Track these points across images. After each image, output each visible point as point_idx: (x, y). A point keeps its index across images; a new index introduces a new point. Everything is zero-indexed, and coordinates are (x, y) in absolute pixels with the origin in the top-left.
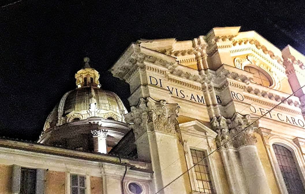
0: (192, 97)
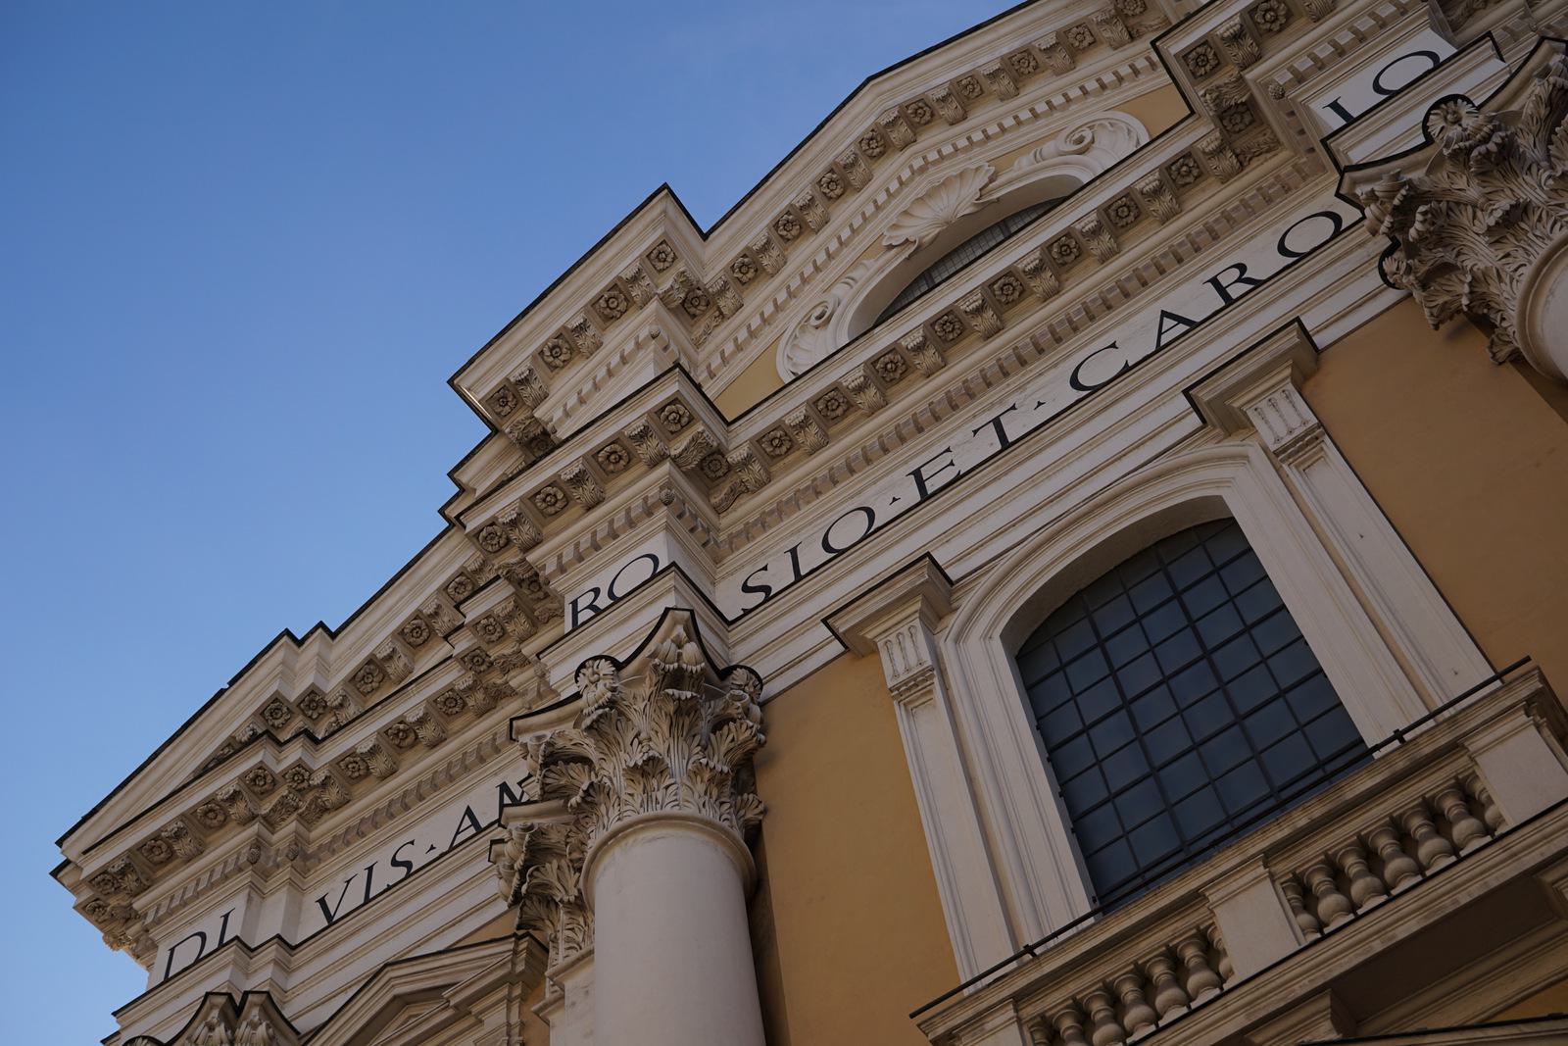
0: (467, 822)
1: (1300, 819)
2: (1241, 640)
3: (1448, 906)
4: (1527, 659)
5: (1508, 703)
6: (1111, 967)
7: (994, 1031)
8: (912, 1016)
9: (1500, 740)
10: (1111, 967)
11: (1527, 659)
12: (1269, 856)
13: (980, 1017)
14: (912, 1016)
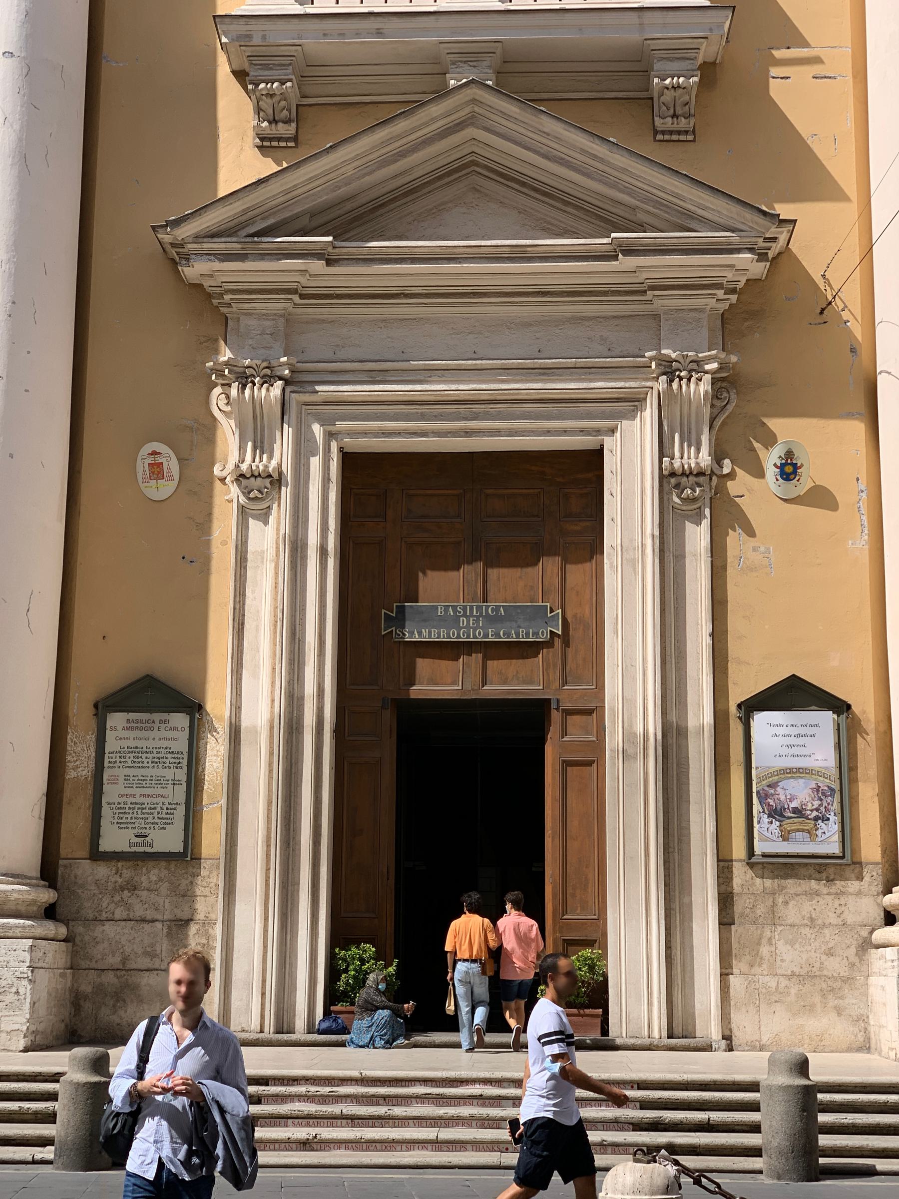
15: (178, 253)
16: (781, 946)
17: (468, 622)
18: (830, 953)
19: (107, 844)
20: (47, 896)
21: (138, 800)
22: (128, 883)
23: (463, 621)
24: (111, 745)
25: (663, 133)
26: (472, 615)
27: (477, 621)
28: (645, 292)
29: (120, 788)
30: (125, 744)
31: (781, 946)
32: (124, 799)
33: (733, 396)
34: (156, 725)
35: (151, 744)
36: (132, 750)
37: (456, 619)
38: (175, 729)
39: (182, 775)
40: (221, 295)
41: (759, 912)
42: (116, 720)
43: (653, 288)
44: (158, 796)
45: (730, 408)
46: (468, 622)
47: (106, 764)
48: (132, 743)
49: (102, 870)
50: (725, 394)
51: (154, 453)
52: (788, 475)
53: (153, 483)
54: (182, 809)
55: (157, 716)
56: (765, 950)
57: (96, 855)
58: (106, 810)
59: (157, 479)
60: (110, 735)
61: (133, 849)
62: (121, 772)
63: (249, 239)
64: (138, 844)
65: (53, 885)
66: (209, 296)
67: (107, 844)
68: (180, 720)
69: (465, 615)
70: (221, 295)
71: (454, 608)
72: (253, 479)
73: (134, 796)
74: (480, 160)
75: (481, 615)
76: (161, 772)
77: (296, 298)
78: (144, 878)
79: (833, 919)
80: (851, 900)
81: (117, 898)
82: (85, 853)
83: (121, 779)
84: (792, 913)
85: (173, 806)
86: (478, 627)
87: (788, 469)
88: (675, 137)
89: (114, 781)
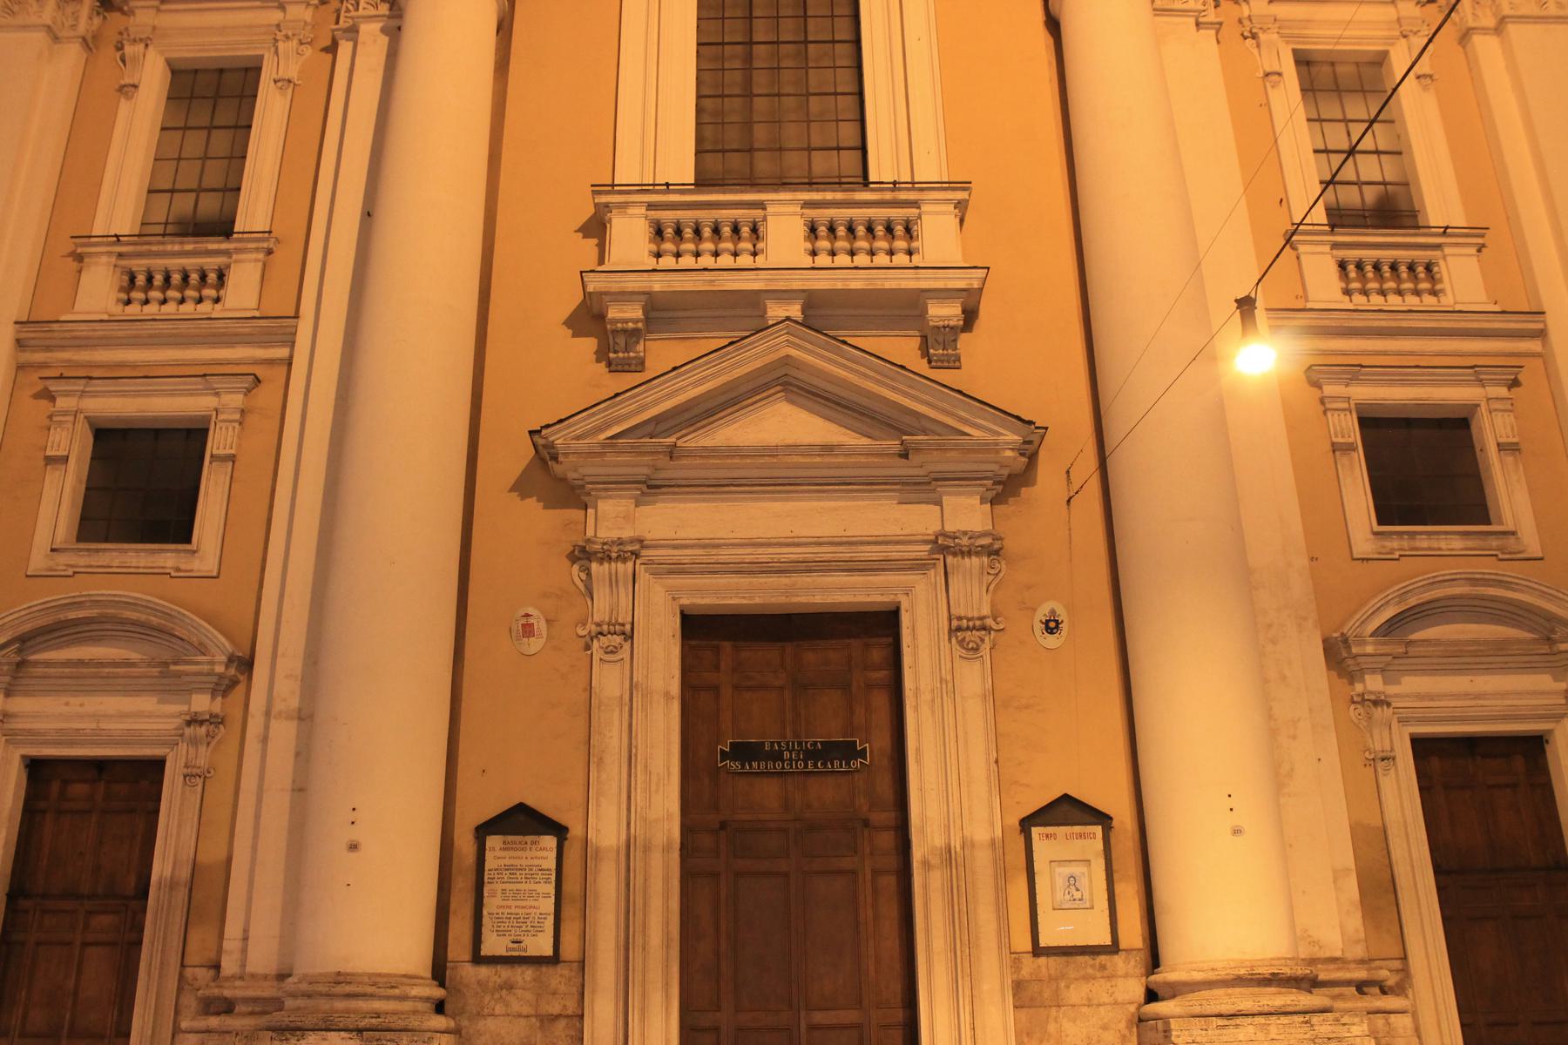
1: (829, 196)
2: (827, 45)
3: (879, 285)
4: (970, 183)
5: (950, 197)
6: (706, 216)
7: (632, 216)
8: (592, 186)
9: (937, 213)
10: (706, 216)
11: (970, 183)
12: (808, 204)
13: (624, 206)
14: (592, 186)
15: (549, 453)
16: (1067, 1026)
17: (791, 755)
18: (1105, 1028)
19: (487, 949)
20: (439, 993)
21: (513, 910)
22: (505, 983)
23: (786, 755)
24: (490, 863)
25: (936, 361)
26: (793, 749)
27: (798, 755)
28: (930, 483)
29: (498, 901)
30: (502, 862)
31: (1067, 1026)
32: (502, 910)
33: (1003, 563)
34: (528, 846)
35: (524, 862)
36: (508, 868)
37: (781, 753)
38: (544, 849)
39: (551, 889)
40: (583, 486)
41: (1046, 995)
42: (493, 842)
43: (936, 480)
44: (531, 907)
45: (1001, 575)
46: (791, 755)
47: (486, 880)
48: (508, 862)
49: (484, 971)
50: (997, 565)
51: (527, 615)
52: (1052, 629)
53: (525, 640)
54: (551, 919)
55: (529, 838)
56: (1052, 1028)
57: (478, 959)
58: (486, 920)
59: (528, 637)
60: (489, 855)
61: (510, 954)
62: (499, 887)
63: (607, 441)
64: (514, 949)
65: (442, 985)
66: (573, 488)
67: (487, 949)
68: (550, 842)
69: (787, 749)
70: (583, 486)
71: (779, 743)
72: (609, 636)
73: (510, 907)
74: (791, 380)
75: (802, 749)
76: (533, 886)
77: (644, 487)
78: (519, 979)
79: (1105, 998)
80: (1120, 982)
81: (497, 996)
82: (467, 956)
83: (499, 892)
84: (1075, 993)
85: (543, 916)
86: (799, 759)
87: (1052, 625)
88: (946, 364)
89: (493, 894)
